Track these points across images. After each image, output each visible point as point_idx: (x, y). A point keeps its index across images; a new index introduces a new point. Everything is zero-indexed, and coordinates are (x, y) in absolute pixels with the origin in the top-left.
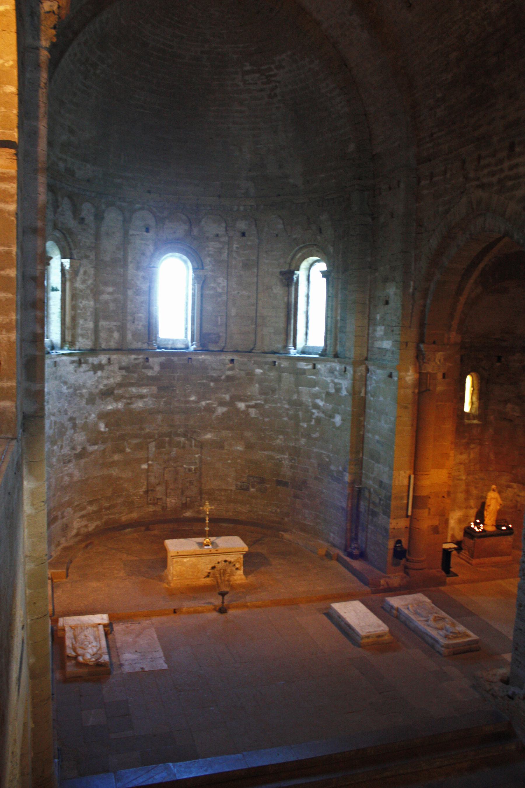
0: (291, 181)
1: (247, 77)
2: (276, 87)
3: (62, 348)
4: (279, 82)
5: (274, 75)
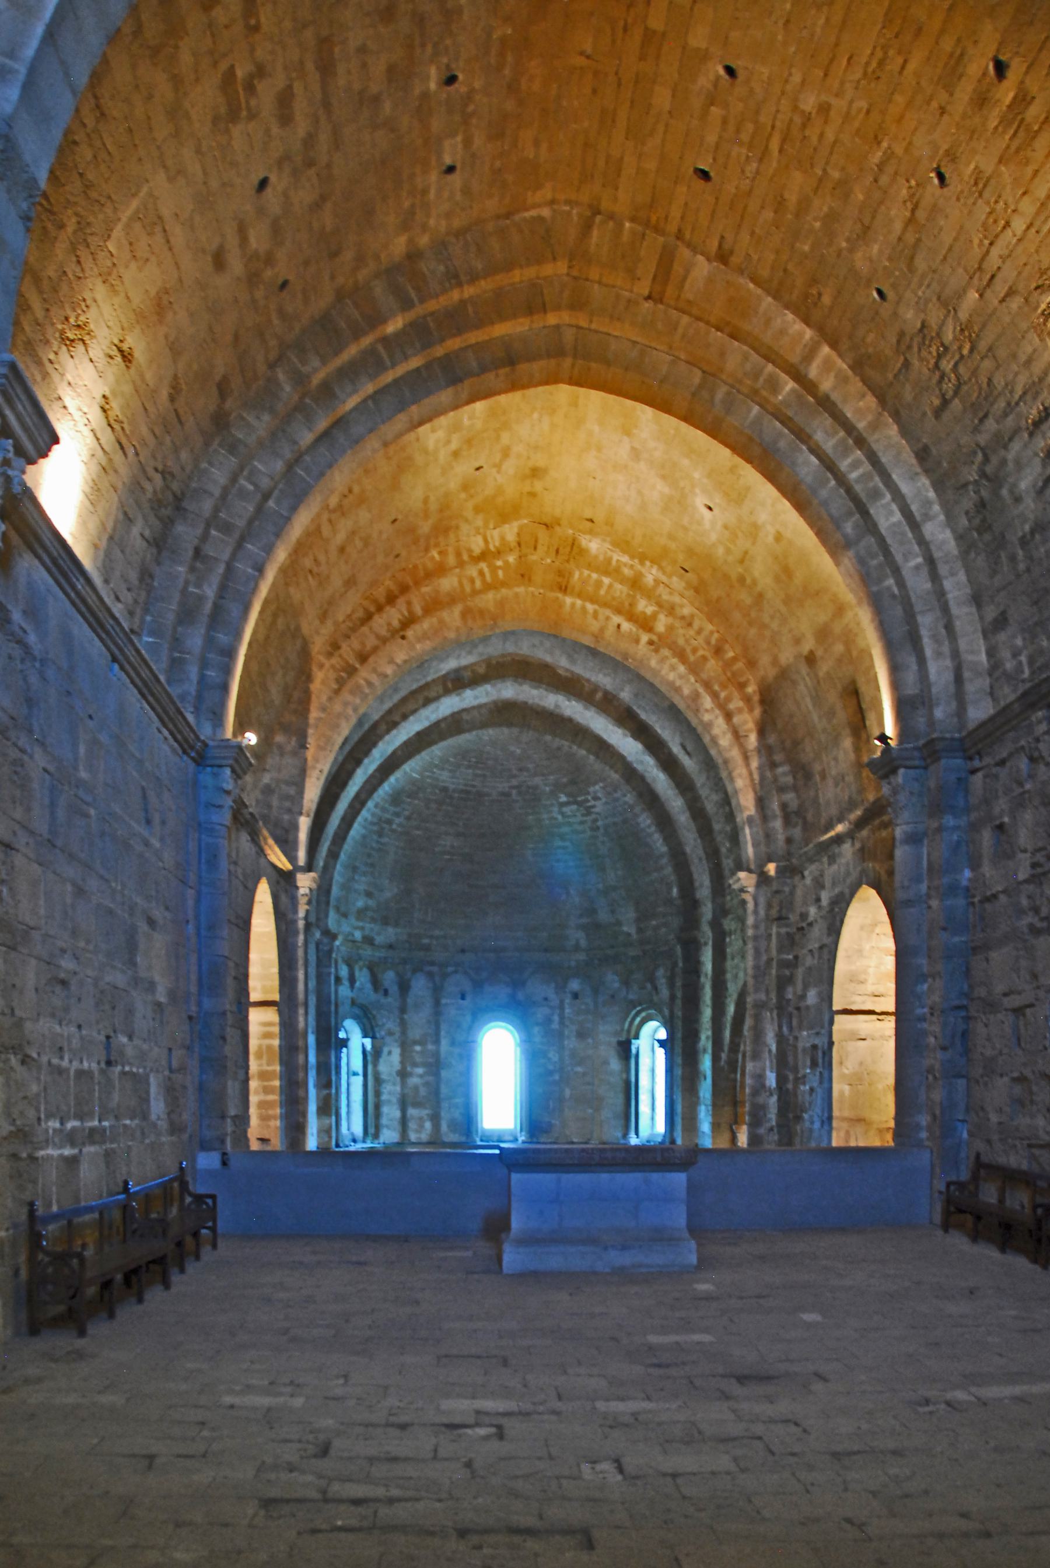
1: (565, 809)
2: (595, 821)
3: (364, 1141)
4: (597, 813)
5: (593, 807)
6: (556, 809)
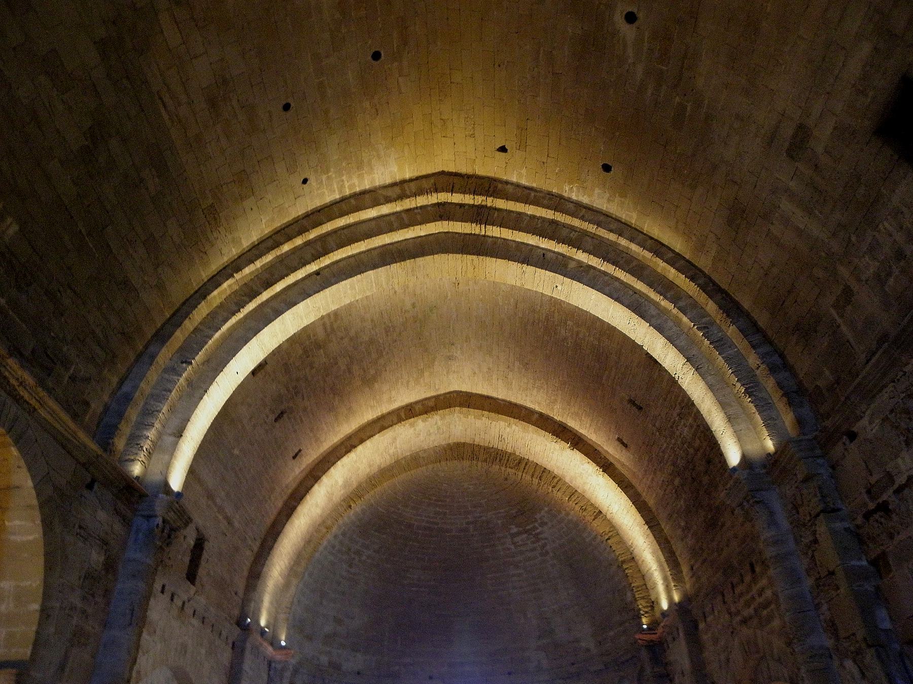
0: (583, 644)
1: (516, 539)
6: (509, 540)
